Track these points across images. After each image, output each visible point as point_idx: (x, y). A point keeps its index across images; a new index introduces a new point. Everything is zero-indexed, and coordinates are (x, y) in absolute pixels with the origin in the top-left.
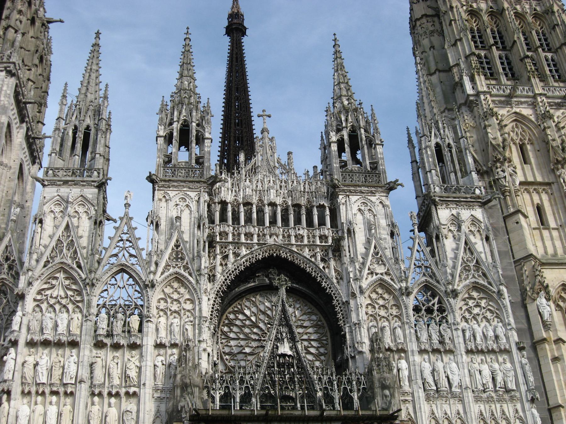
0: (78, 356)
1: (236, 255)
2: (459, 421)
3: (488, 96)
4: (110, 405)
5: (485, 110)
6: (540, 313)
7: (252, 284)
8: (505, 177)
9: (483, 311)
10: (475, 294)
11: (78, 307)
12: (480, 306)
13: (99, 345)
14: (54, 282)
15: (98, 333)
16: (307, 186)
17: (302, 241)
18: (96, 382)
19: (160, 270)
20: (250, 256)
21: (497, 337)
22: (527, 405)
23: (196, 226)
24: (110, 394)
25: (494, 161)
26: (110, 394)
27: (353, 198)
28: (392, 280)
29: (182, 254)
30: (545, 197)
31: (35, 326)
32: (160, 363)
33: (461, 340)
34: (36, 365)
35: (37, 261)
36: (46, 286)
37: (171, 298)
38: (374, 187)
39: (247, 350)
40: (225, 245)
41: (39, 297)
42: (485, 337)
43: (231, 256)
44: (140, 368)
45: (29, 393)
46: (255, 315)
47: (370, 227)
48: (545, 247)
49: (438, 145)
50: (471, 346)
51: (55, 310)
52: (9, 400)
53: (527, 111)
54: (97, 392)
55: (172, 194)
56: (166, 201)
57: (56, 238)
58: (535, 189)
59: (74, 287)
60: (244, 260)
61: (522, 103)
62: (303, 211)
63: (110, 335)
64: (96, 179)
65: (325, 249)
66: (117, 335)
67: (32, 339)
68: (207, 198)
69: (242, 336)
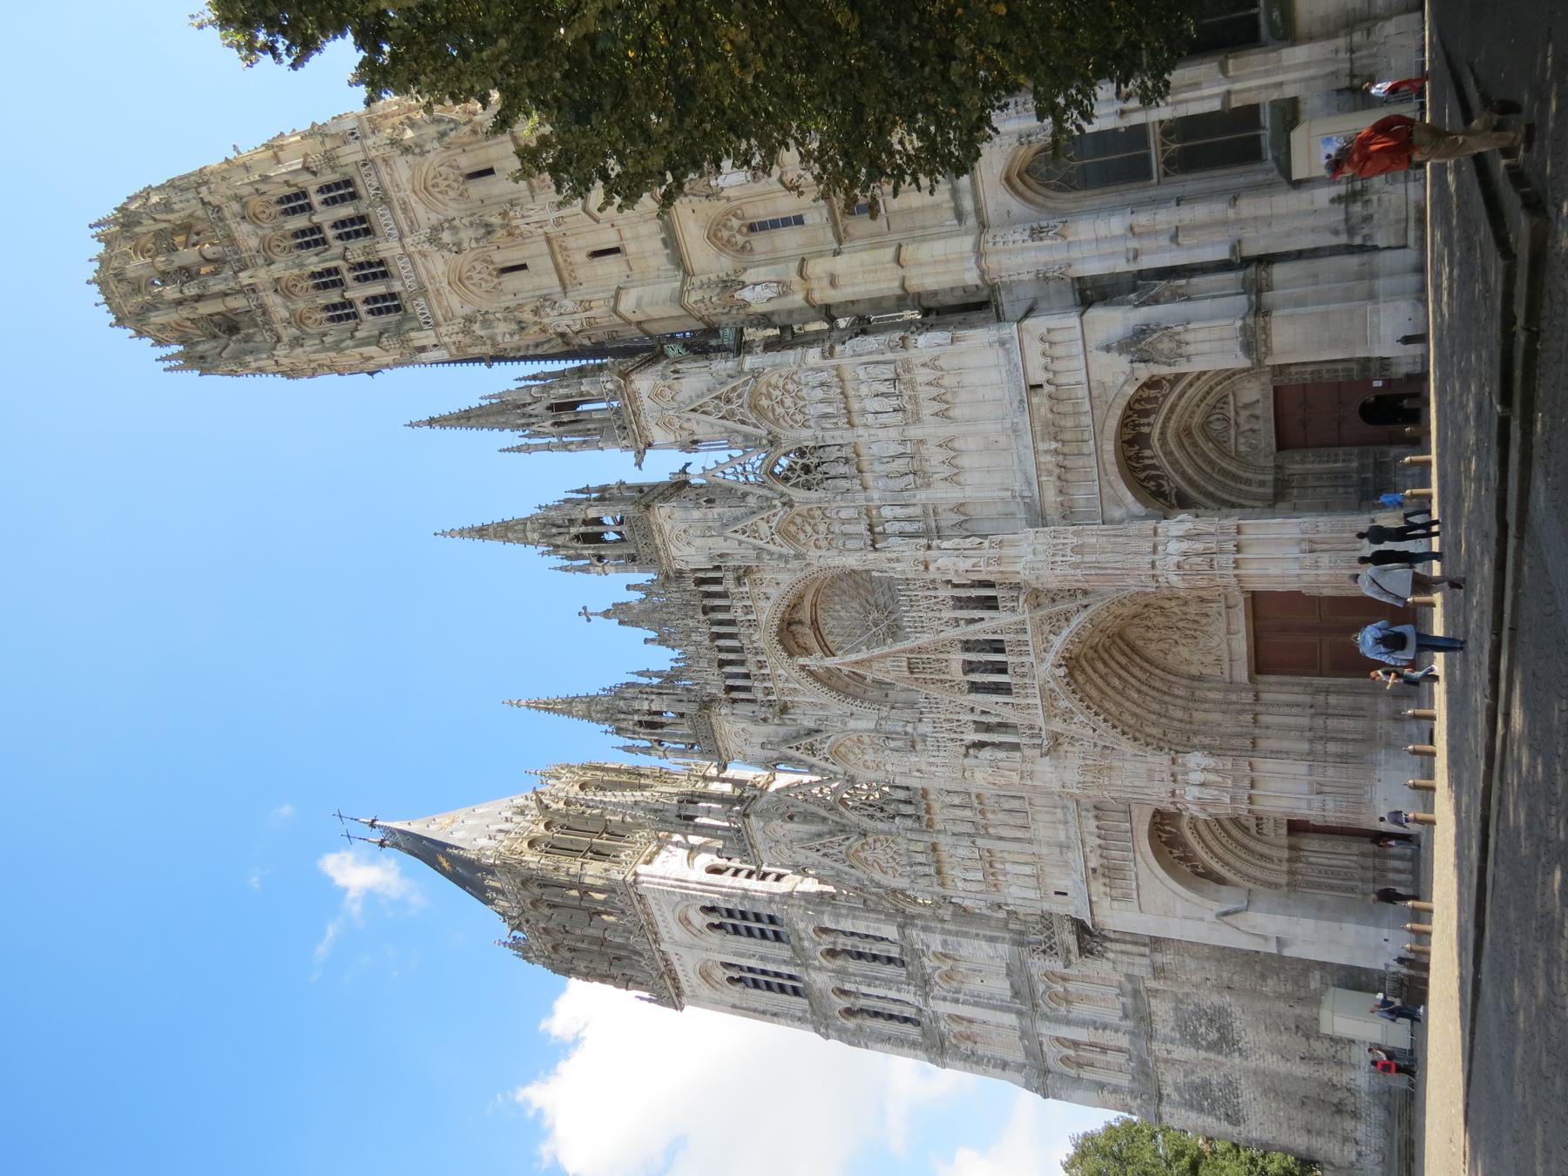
2: (950, 445)
3: (443, 330)
10: (764, 402)
13: (930, 825)
14: (870, 858)
18: (973, 831)
19: (831, 767)
20: (785, 665)
22: (912, 351)
27: (674, 551)
28: (774, 515)
33: (837, 433)
41: (890, 871)
43: (791, 686)
49: (555, 424)
52: (1006, 904)
54: (982, 832)
57: (821, 859)
61: (428, 272)
62: (707, 602)
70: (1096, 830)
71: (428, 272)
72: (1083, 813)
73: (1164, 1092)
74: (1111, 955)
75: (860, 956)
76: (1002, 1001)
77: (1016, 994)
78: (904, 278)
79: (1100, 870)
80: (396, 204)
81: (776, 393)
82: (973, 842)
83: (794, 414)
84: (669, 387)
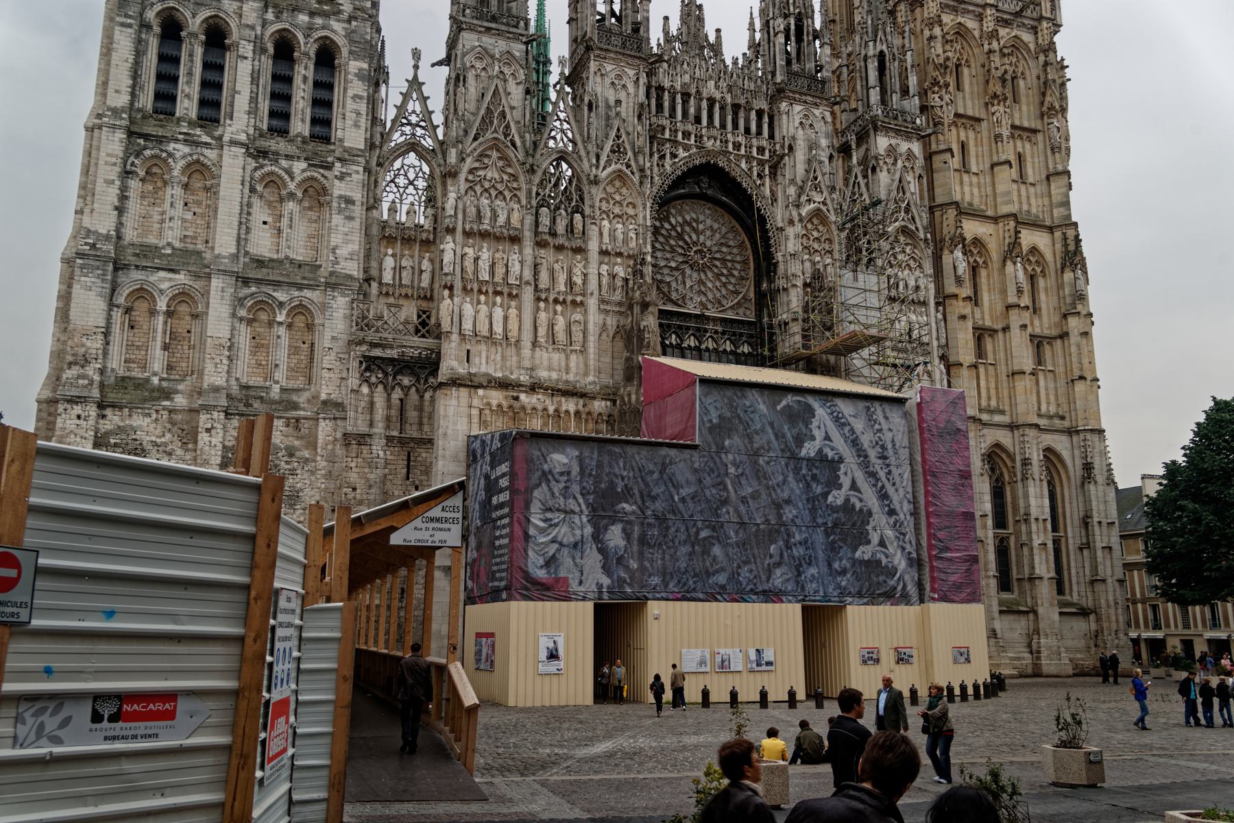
0: (521, 253)
1: (674, 156)
4: (555, 313)
5: (932, 15)
6: (955, 267)
7: (682, 191)
8: (941, 107)
9: (907, 257)
10: (902, 239)
11: (515, 195)
12: (904, 252)
14: (486, 161)
15: (540, 229)
16: (746, 82)
17: (738, 150)
18: (542, 286)
21: (917, 288)
22: (937, 361)
23: (636, 114)
24: (556, 301)
25: (932, 84)
26: (556, 301)
27: (798, 108)
29: (625, 148)
30: (971, 134)
31: (472, 211)
32: (605, 273)
34: (477, 259)
35: (466, 132)
36: (477, 165)
37: (613, 199)
38: (819, 98)
39: (673, 264)
40: (662, 143)
41: (470, 177)
42: (906, 286)
43: (668, 156)
44: (585, 275)
45: (472, 289)
46: (681, 225)
47: (812, 146)
48: (963, 193)
50: (893, 293)
51: (490, 195)
52: (451, 296)
53: (971, 24)
54: (543, 296)
55: (609, 68)
56: (602, 75)
58: (963, 124)
59: (509, 170)
60: (681, 163)
61: (969, 12)
62: (742, 114)
63: (553, 234)
64: (524, 32)
65: (761, 163)
66: (563, 235)
67: (472, 228)
68: (646, 81)
69: (667, 248)
70: (564, 408)
71: (969, 12)
72: (581, 402)
73: (108, 412)
74: (365, 390)
75: (282, 80)
76: (246, 240)
77: (260, 263)
78: (961, 365)
79: (516, 404)
80: (1012, 18)
81: (908, 249)
82: (528, 283)
83: (896, 258)
84: (912, 168)
